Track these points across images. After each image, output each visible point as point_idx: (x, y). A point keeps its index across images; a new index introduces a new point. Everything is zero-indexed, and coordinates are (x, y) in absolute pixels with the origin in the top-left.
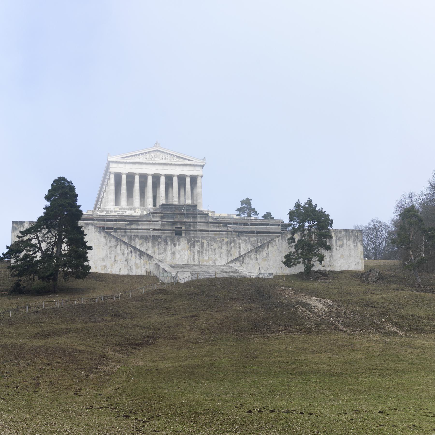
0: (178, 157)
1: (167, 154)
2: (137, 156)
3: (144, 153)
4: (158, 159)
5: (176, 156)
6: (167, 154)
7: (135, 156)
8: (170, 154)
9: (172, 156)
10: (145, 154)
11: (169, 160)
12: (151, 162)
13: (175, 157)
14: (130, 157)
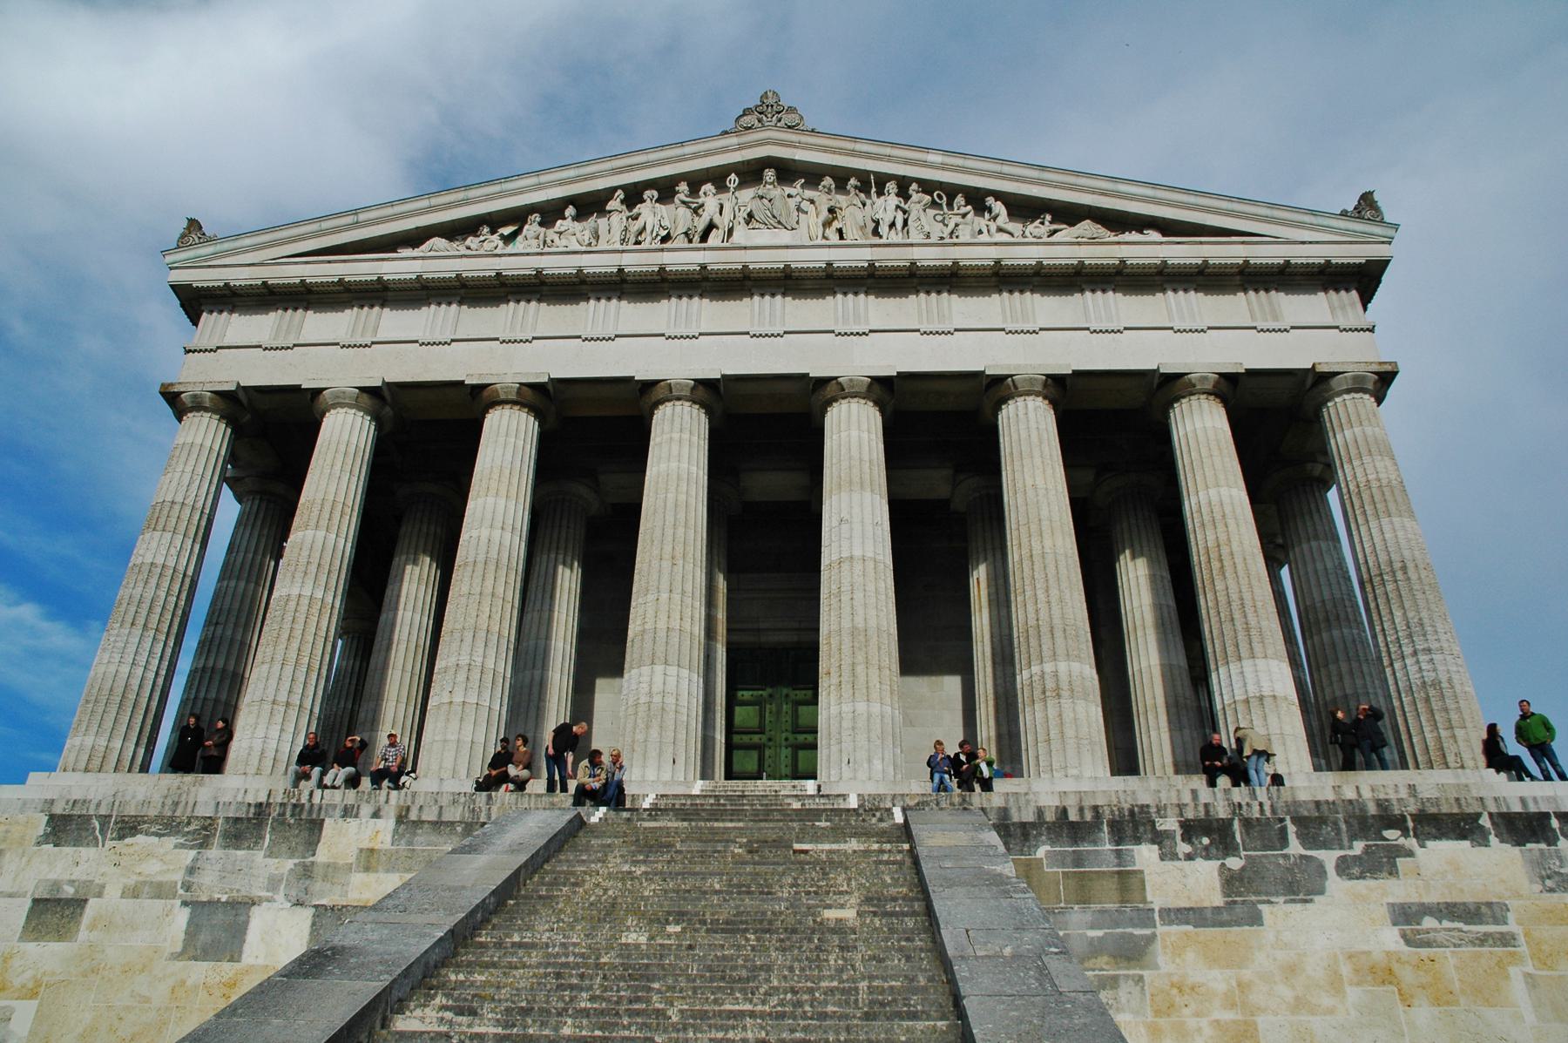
0: (1024, 209)
1: (891, 187)
2: (532, 228)
3: (611, 191)
4: (784, 237)
5: (999, 196)
6: (891, 187)
7: (507, 231)
8: (927, 186)
9: (960, 200)
10: (611, 205)
11: (916, 237)
12: (683, 259)
13: (999, 207)
14: (438, 242)
